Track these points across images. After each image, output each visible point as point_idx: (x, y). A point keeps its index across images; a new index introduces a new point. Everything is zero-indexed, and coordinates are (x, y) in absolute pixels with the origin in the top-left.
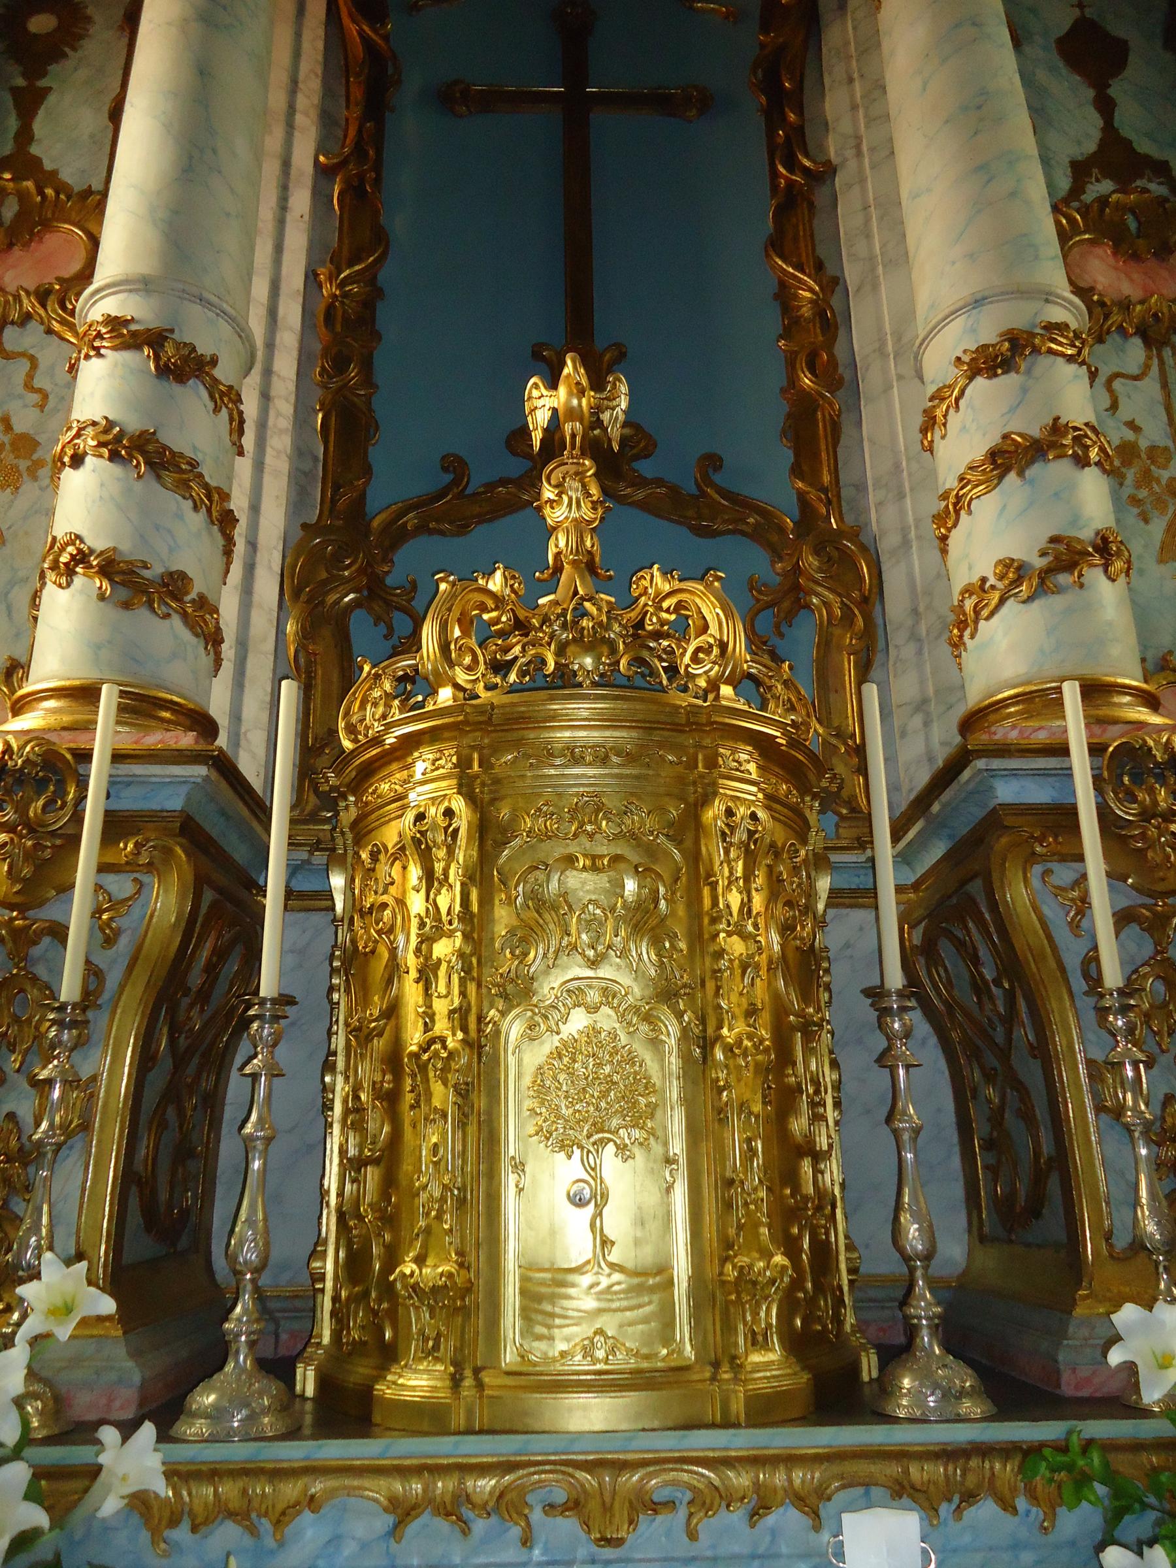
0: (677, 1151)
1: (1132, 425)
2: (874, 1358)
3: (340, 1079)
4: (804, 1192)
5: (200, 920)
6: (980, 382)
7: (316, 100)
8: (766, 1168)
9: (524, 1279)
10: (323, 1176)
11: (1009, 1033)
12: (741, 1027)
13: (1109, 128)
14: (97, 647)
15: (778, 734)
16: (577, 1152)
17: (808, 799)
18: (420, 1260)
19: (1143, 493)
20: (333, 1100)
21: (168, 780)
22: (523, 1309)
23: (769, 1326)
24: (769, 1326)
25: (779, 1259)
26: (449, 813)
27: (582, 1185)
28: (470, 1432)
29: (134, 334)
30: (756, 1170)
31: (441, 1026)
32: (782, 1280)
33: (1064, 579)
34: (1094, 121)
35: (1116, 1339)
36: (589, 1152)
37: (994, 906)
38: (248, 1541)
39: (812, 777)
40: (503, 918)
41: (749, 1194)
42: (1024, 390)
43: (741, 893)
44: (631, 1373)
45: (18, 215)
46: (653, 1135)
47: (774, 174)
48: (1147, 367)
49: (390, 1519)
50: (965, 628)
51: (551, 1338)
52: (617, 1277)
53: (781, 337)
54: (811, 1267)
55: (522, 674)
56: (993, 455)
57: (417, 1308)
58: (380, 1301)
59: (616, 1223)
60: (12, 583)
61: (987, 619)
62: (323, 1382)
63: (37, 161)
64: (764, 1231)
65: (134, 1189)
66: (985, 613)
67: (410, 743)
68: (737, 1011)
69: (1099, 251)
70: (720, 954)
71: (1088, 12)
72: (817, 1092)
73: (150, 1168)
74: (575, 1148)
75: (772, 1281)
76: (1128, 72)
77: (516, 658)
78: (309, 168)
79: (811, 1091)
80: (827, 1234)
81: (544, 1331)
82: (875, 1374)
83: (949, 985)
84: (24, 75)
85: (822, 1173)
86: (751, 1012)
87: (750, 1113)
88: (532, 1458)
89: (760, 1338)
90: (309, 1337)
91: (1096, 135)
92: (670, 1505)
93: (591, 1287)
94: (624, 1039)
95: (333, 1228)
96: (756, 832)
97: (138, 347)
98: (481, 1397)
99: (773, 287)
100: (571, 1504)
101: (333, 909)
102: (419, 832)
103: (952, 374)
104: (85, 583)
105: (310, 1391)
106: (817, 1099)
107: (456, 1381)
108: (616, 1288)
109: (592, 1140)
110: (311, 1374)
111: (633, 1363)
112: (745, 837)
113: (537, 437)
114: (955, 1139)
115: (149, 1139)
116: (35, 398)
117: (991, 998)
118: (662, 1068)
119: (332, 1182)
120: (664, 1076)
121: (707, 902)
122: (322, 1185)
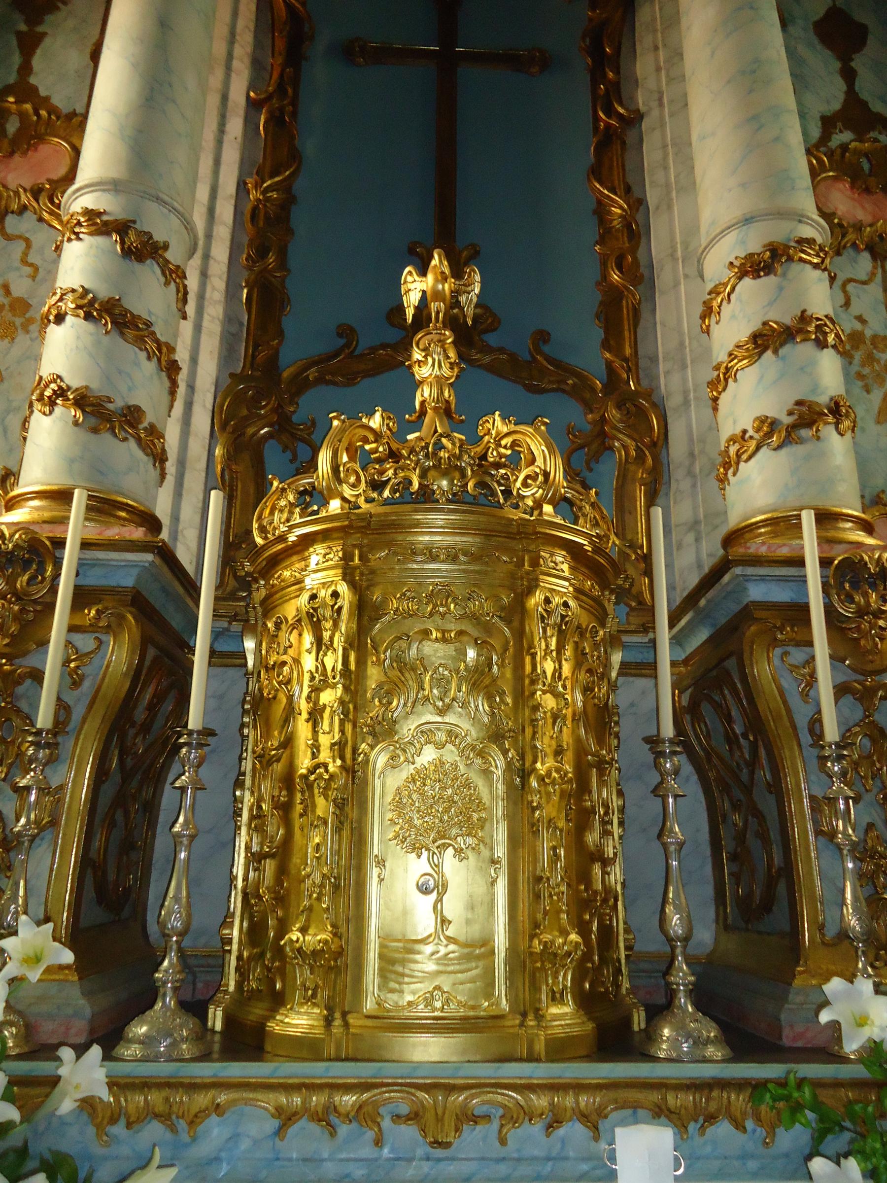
0: (500, 855)
1: (860, 319)
2: (643, 1014)
3: (247, 794)
4: (595, 888)
5: (144, 673)
6: (747, 281)
7: (249, 49)
8: (566, 869)
9: (382, 946)
10: (233, 865)
11: (752, 773)
12: (550, 762)
13: (851, 93)
14: (71, 461)
15: (586, 543)
16: (425, 854)
17: (607, 593)
18: (304, 930)
19: (866, 371)
20: (241, 809)
21: (123, 564)
22: (381, 969)
23: (565, 987)
24: (565, 987)
25: (574, 937)
26: (335, 595)
27: (428, 877)
28: (338, 1059)
29: (105, 223)
30: (559, 870)
31: (325, 755)
32: (576, 953)
33: (805, 433)
35: (825, 1003)
36: (434, 853)
37: (744, 678)
38: (168, 1135)
39: (610, 575)
40: (374, 675)
41: (553, 888)
42: (781, 289)
43: (554, 662)
44: (460, 1019)
45: (19, 130)
46: (483, 842)
47: (596, 119)
48: (873, 274)
49: (276, 1123)
50: (729, 468)
51: (401, 992)
52: (452, 947)
53: (597, 243)
54: (598, 944)
55: (393, 491)
56: (755, 337)
57: (300, 966)
58: (273, 960)
59: (453, 907)
61: (746, 461)
62: (228, 1020)
63: (35, 89)
64: (564, 916)
65: (89, 871)
66: (745, 457)
67: (307, 541)
68: (548, 750)
70: (536, 708)
72: (606, 813)
73: (102, 857)
74: (423, 850)
75: (568, 954)
76: (866, 50)
77: (390, 479)
78: (242, 101)
79: (602, 813)
80: (611, 920)
81: (397, 986)
82: (643, 1026)
83: (708, 736)
84: (28, 22)
85: (609, 874)
86: (559, 752)
87: (556, 828)
88: (385, 1081)
89: (558, 996)
90: (218, 987)
91: (842, 97)
92: (487, 1117)
93: (433, 954)
94: (462, 768)
95: (239, 905)
96: (567, 616)
97: (108, 234)
98: (347, 1034)
99: (593, 205)
100: (412, 1116)
101: (246, 665)
102: (313, 608)
103: (727, 274)
104: (64, 412)
105: (218, 1027)
106: (606, 819)
107: (328, 1021)
108: (451, 955)
109: (437, 844)
110: (219, 1014)
111: (462, 1012)
112: (559, 620)
113: (410, 313)
114: (708, 851)
115: (102, 834)
116: (28, 270)
117: (740, 747)
118: (491, 792)
119: (239, 870)
120: (492, 798)
121: (528, 668)
122: (231, 872)
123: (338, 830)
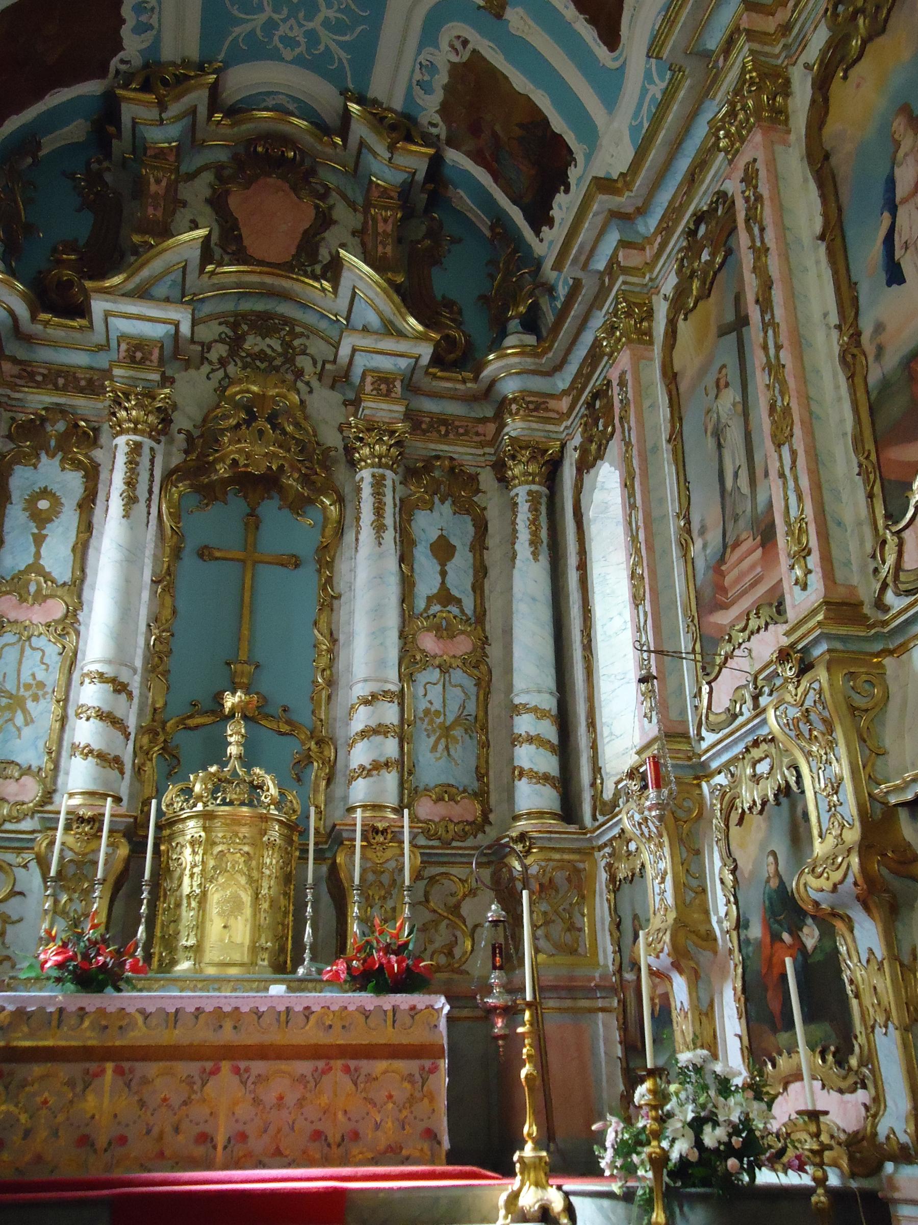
6: (362, 706)
13: (443, 583)
14: (95, 779)
18: (187, 940)
25: (269, 944)
33: (375, 772)
34: (439, 579)
42: (374, 712)
60: (37, 738)
63: (43, 567)
69: (430, 634)
71: (444, 533)
76: (454, 560)
78: (149, 582)
84: (37, 527)
86: (270, 888)
91: (438, 586)
107: (195, 964)
113: (227, 710)
116: (44, 667)
123: (199, 911)
